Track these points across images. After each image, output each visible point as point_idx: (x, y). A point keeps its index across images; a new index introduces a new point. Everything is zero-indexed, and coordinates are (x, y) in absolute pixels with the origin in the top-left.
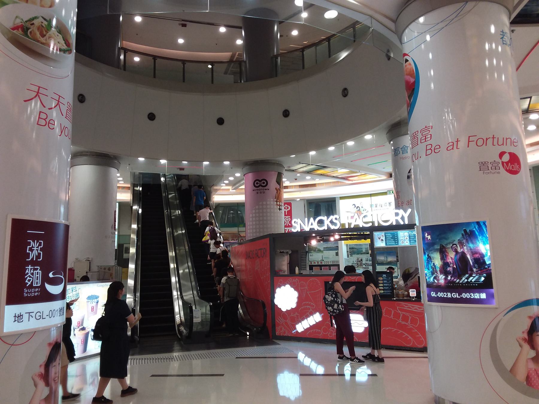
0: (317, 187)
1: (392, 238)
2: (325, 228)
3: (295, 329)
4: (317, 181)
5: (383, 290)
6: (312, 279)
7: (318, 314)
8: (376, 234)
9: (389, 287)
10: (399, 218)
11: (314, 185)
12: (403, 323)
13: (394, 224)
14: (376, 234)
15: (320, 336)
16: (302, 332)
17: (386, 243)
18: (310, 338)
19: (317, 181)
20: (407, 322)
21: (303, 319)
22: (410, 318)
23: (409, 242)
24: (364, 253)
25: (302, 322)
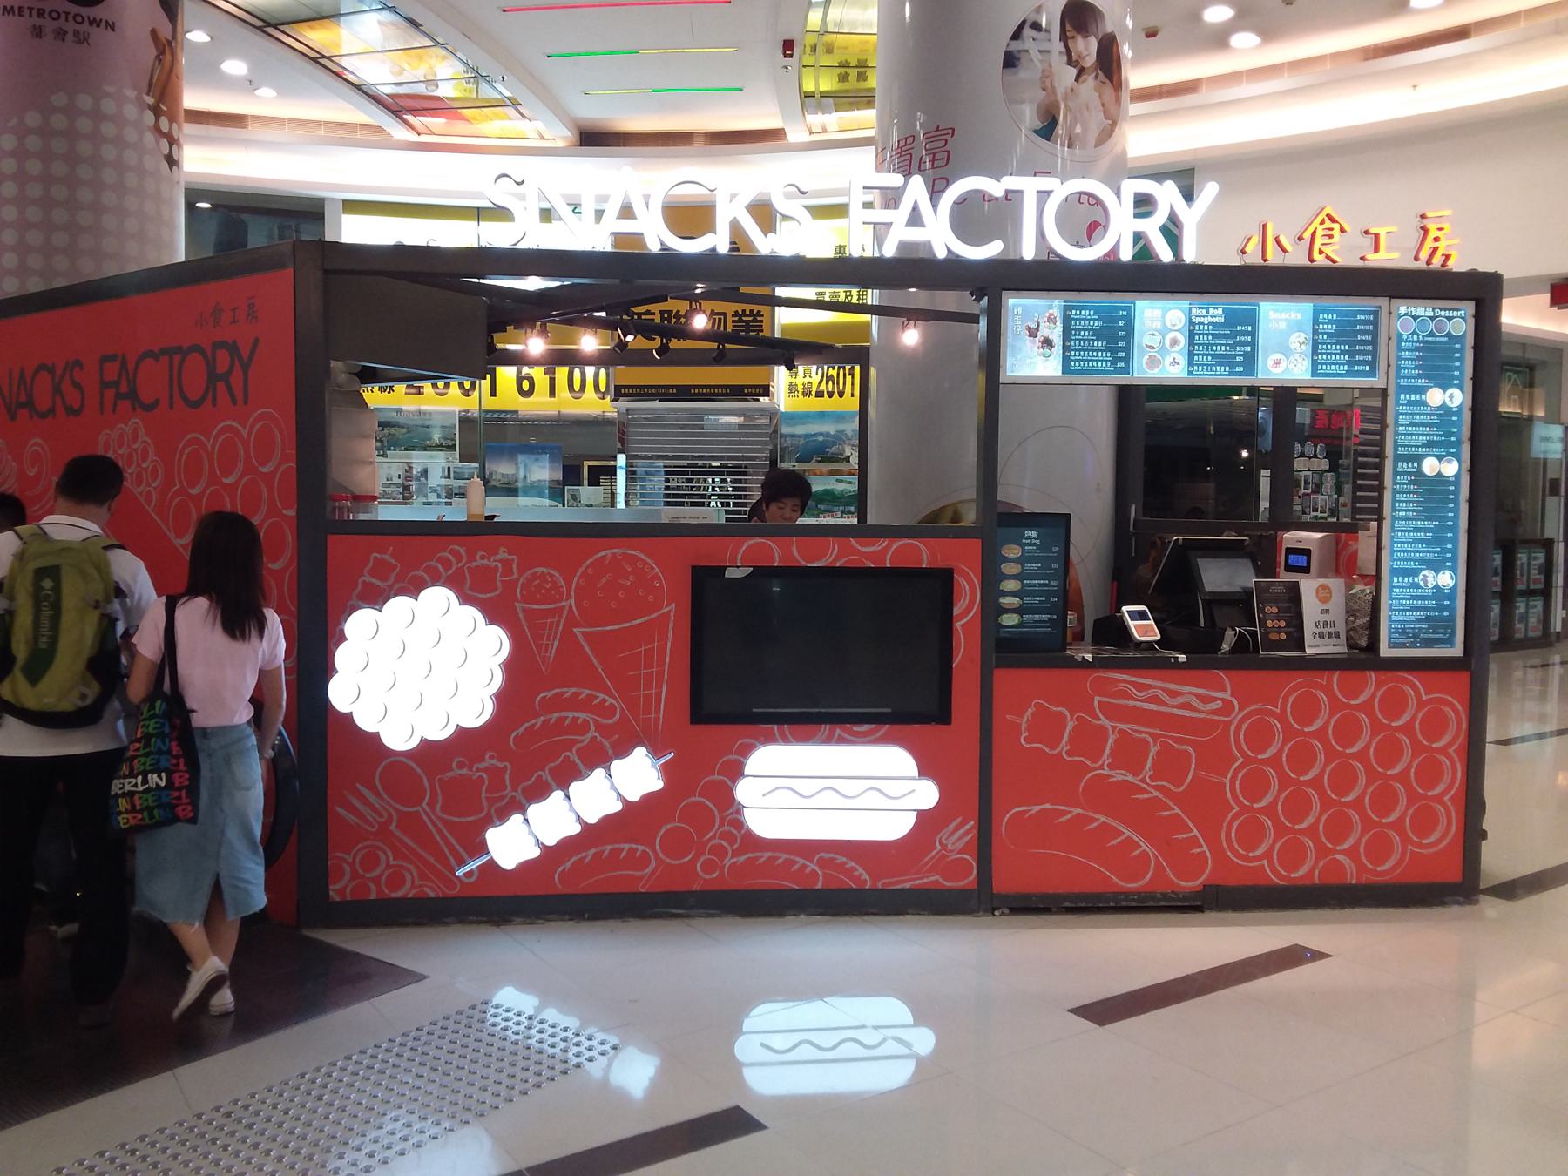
0: (252, 132)
1: (1099, 335)
2: (718, 241)
3: (483, 848)
4: (264, 102)
5: (1019, 611)
6: (610, 551)
7: (640, 753)
8: (1019, 307)
9: (1048, 594)
10: (1152, 227)
11: (236, 120)
12: (1119, 776)
13: (1126, 254)
14: (1019, 307)
15: (645, 879)
16: (526, 867)
17: (1066, 362)
18: (583, 893)
19: (264, 102)
20: (1136, 769)
21: (539, 793)
22: (1153, 750)
23: (1183, 361)
24: (439, 447)
25: (534, 810)
